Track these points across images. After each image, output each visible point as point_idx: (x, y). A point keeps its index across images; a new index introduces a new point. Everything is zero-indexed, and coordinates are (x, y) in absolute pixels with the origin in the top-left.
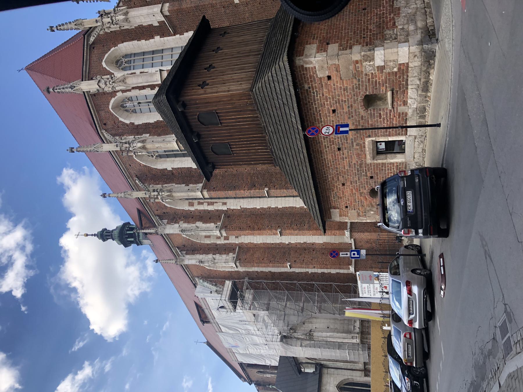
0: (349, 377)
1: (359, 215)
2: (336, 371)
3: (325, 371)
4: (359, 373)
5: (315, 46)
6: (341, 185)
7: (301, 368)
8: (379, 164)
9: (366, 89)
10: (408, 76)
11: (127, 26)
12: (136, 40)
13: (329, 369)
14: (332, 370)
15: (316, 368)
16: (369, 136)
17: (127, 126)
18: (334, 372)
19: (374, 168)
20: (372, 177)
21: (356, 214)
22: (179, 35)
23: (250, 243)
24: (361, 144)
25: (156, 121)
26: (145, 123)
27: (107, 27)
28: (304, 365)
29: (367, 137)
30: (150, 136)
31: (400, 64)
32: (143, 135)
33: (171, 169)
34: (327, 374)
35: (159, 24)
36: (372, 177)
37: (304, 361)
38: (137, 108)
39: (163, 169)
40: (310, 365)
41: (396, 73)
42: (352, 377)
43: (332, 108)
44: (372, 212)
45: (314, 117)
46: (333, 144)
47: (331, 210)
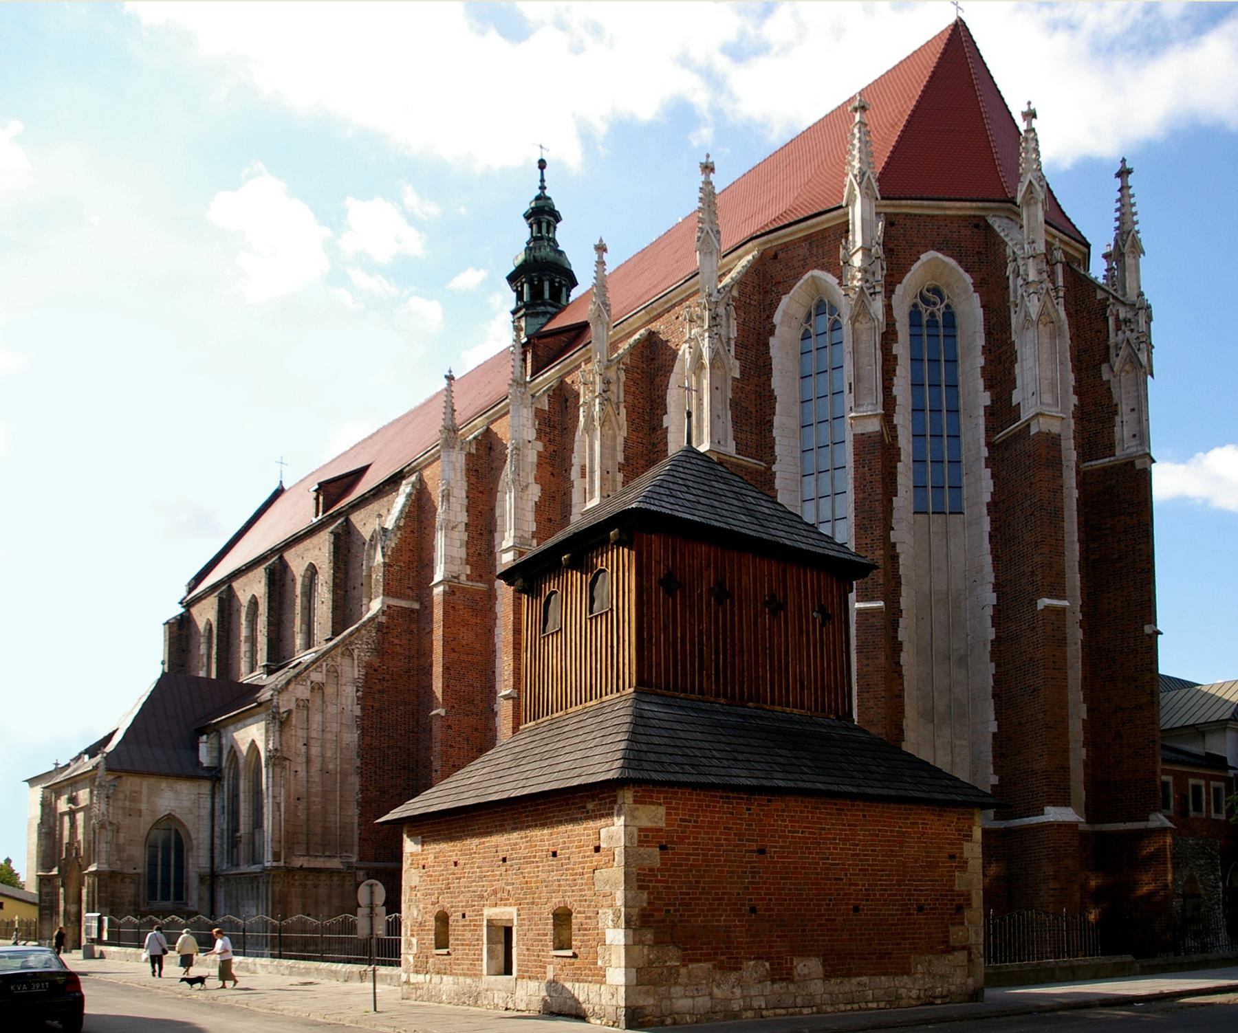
0: (195, 842)
1: (413, 888)
2: (205, 812)
3: (205, 787)
4: (204, 862)
5: (662, 824)
6: (455, 859)
7: (208, 734)
8: (482, 930)
9: (579, 912)
10: (590, 982)
11: (1017, 322)
12: (986, 340)
13: (209, 798)
14: (208, 805)
15: (209, 769)
16: (519, 915)
17: (768, 317)
18: (205, 808)
19: (476, 920)
20: (464, 916)
21: (413, 885)
22: (987, 455)
23: (495, 619)
24: (508, 899)
25: (776, 394)
26: (771, 364)
27: (1018, 267)
28: (214, 741)
29: (518, 910)
30: (734, 379)
31: (603, 969)
32: (737, 363)
33: (664, 426)
34: (199, 794)
35: (1016, 406)
36: (464, 916)
37: (224, 741)
38: (812, 344)
39: (665, 405)
40: (215, 754)
41: (596, 963)
42: (195, 848)
43: (558, 852)
44: (415, 914)
45: (550, 818)
46: (512, 849)
47: (420, 837)
